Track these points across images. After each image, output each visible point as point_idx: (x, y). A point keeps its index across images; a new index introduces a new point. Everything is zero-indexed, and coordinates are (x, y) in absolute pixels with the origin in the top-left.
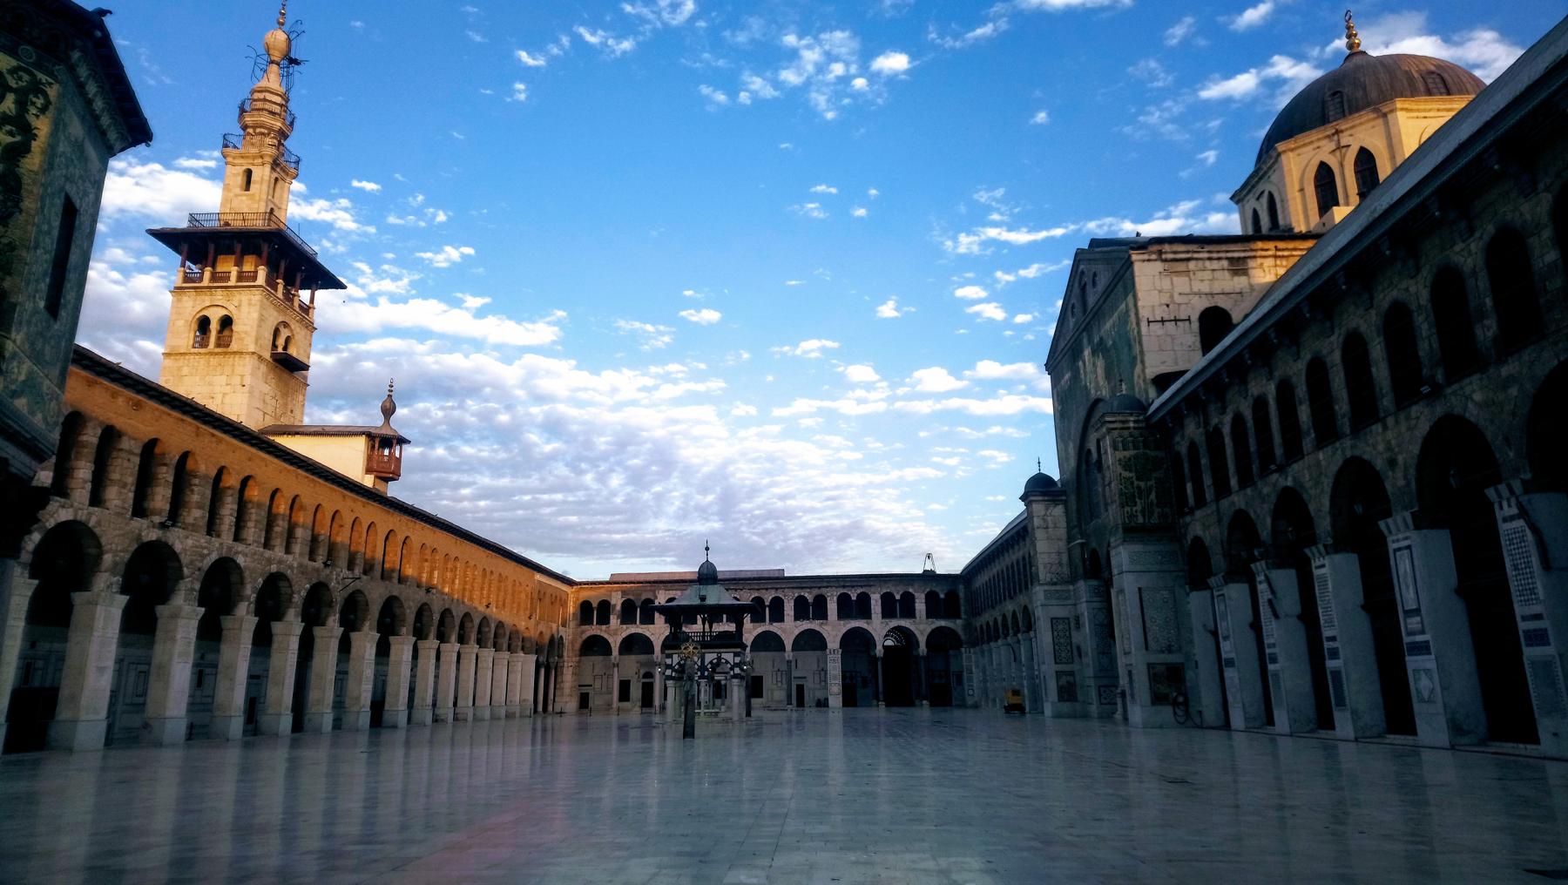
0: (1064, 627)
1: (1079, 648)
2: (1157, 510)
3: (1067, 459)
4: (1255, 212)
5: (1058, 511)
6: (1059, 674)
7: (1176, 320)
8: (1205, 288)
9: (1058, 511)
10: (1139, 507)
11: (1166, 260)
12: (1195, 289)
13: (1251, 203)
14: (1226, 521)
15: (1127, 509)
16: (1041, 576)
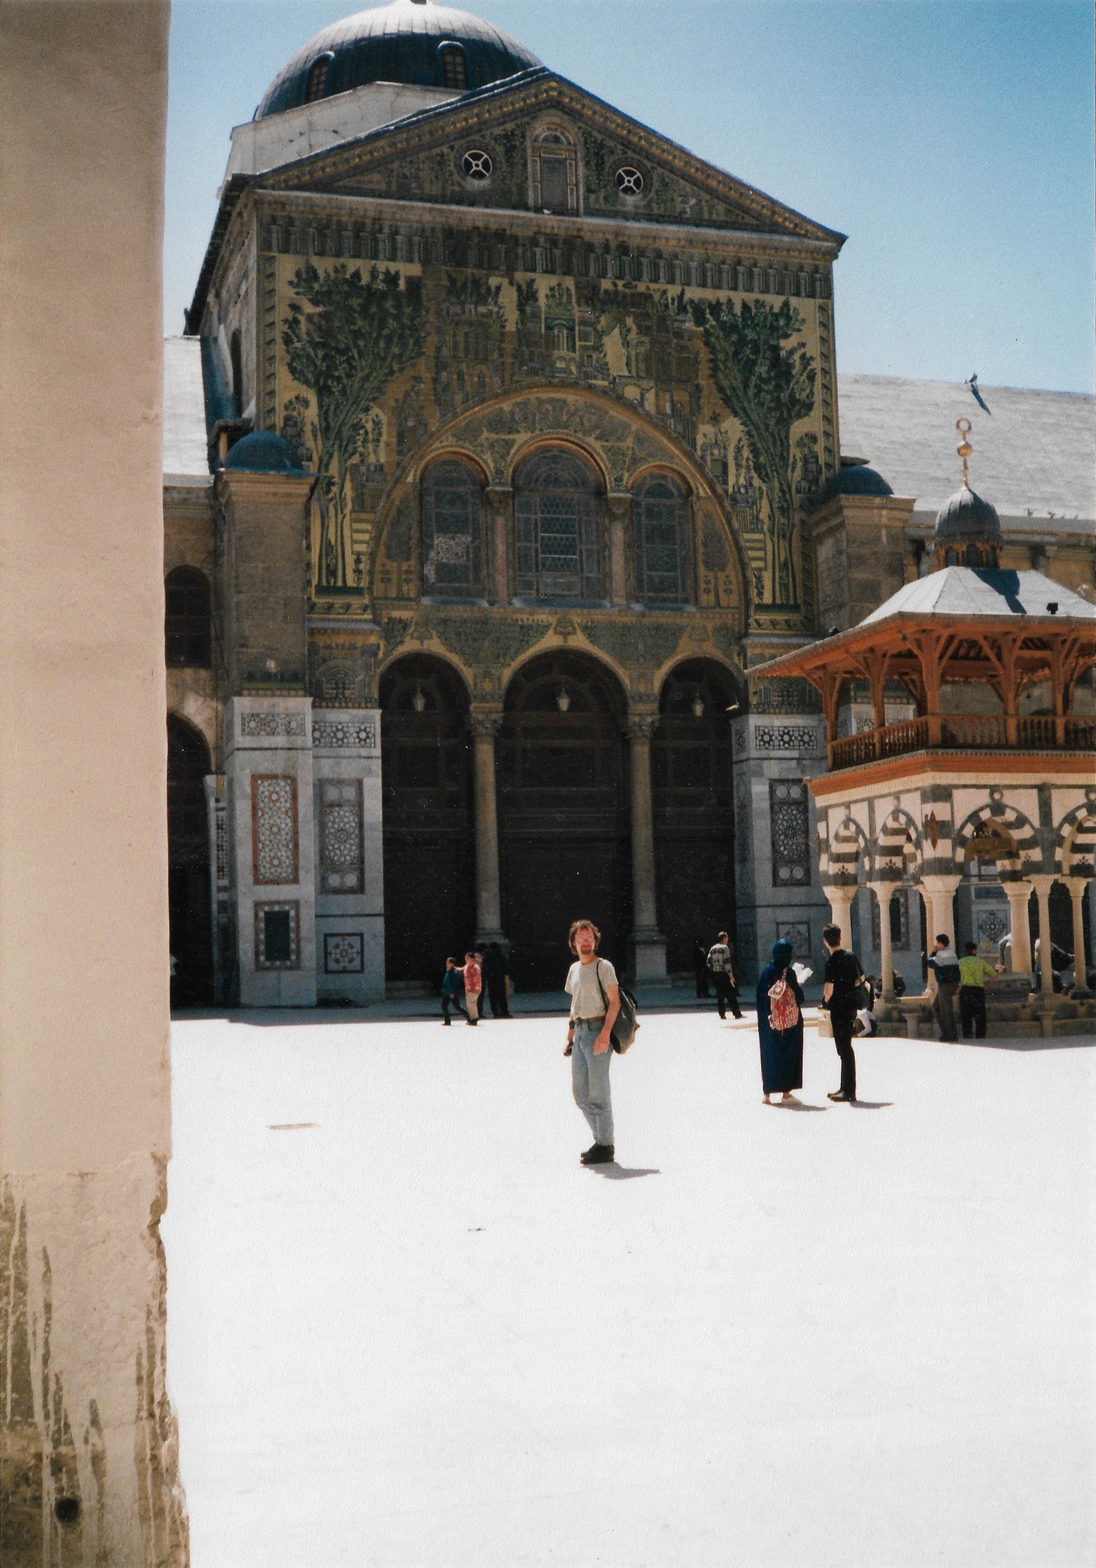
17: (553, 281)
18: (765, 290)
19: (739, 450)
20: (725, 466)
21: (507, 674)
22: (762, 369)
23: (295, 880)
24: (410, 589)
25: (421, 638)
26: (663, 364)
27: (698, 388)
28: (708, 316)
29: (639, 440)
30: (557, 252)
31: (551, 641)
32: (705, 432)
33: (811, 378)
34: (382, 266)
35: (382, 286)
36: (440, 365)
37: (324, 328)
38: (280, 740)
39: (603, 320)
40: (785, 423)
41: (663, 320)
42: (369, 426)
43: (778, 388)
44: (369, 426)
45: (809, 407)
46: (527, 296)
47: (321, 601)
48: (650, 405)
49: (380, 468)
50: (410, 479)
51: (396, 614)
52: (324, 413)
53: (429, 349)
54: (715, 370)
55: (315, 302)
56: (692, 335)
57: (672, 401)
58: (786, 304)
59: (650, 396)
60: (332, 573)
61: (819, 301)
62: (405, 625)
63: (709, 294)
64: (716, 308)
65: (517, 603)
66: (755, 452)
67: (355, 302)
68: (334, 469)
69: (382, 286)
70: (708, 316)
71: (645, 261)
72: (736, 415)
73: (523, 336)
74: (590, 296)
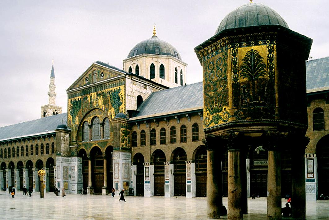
0: (66, 169)
1: (70, 175)
2: (128, 144)
3: (73, 121)
4: (130, 67)
5: (68, 136)
6: (64, 182)
7: (133, 96)
8: (139, 90)
9: (68, 136)
10: (124, 143)
11: (132, 80)
12: (137, 90)
13: (129, 64)
14: (153, 151)
15: (122, 143)
16: (62, 154)
17: (94, 93)
18: (117, 86)
19: (113, 113)
20: (111, 116)
21: (90, 151)
22: (116, 99)
23: (60, 179)
24: (81, 140)
25: (82, 147)
26: (105, 103)
27: (109, 105)
28: (110, 93)
29: (104, 114)
30: (94, 89)
31: (94, 146)
32: (109, 111)
33: (122, 99)
34: (78, 97)
35: (78, 100)
36: (83, 110)
37: (73, 108)
38: (59, 162)
39: (99, 97)
40: (119, 107)
41: (105, 95)
42: (76, 119)
43: (118, 101)
44: (76, 119)
45: (122, 103)
46: (91, 97)
47: (72, 143)
48: (103, 109)
49: (77, 125)
50: (81, 126)
51: (80, 144)
52: (72, 119)
53: (82, 107)
54: (111, 101)
55: (72, 104)
56: (108, 96)
57: (106, 108)
58: (120, 88)
59: (104, 107)
60: (73, 140)
61: (124, 85)
62: (80, 145)
63: (110, 89)
64: (111, 91)
65: (91, 141)
66: (115, 113)
67: (75, 103)
68: (73, 126)
69: (78, 100)
70: (110, 93)
71: (103, 87)
72: (113, 107)
73: (91, 103)
74: (98, 95)
